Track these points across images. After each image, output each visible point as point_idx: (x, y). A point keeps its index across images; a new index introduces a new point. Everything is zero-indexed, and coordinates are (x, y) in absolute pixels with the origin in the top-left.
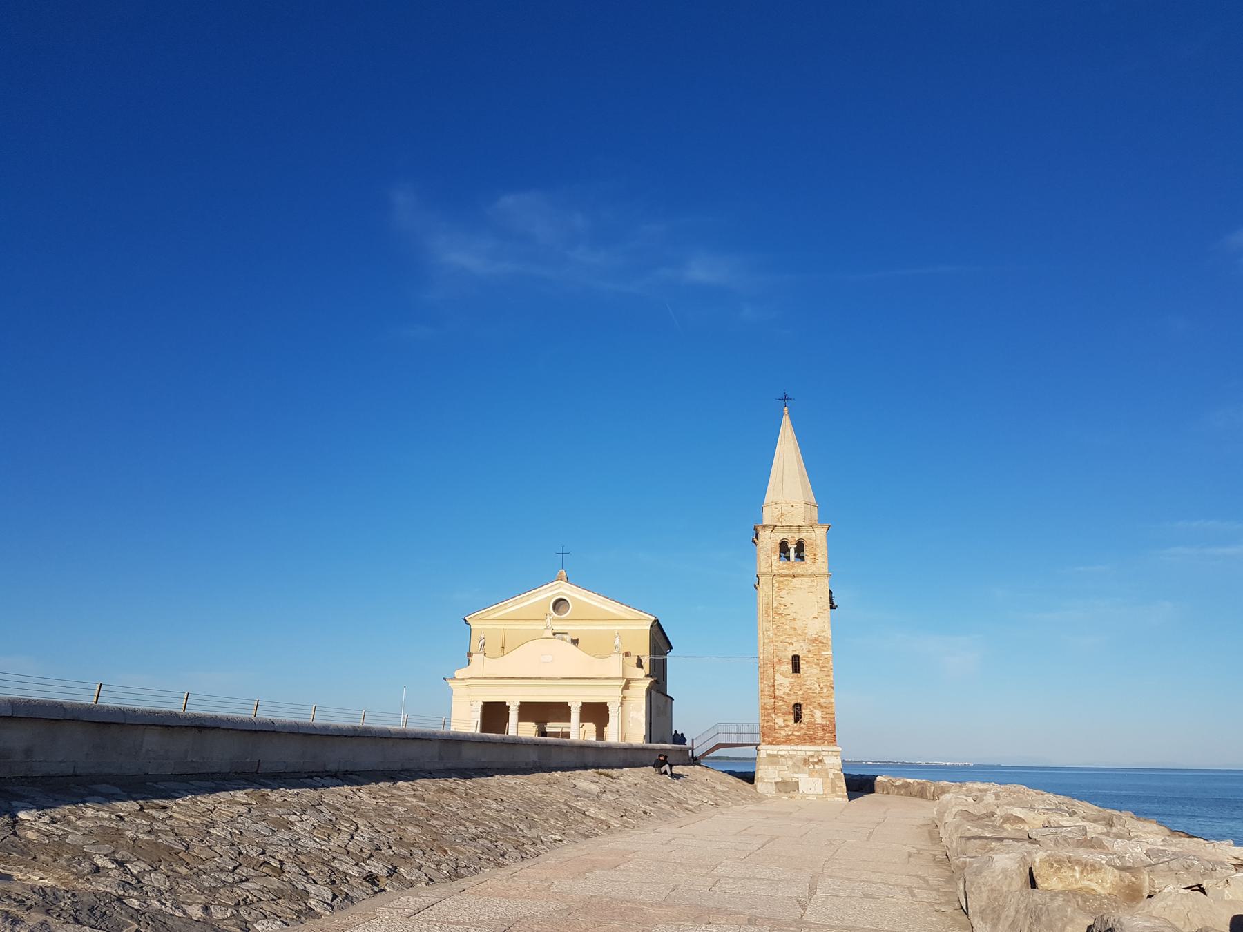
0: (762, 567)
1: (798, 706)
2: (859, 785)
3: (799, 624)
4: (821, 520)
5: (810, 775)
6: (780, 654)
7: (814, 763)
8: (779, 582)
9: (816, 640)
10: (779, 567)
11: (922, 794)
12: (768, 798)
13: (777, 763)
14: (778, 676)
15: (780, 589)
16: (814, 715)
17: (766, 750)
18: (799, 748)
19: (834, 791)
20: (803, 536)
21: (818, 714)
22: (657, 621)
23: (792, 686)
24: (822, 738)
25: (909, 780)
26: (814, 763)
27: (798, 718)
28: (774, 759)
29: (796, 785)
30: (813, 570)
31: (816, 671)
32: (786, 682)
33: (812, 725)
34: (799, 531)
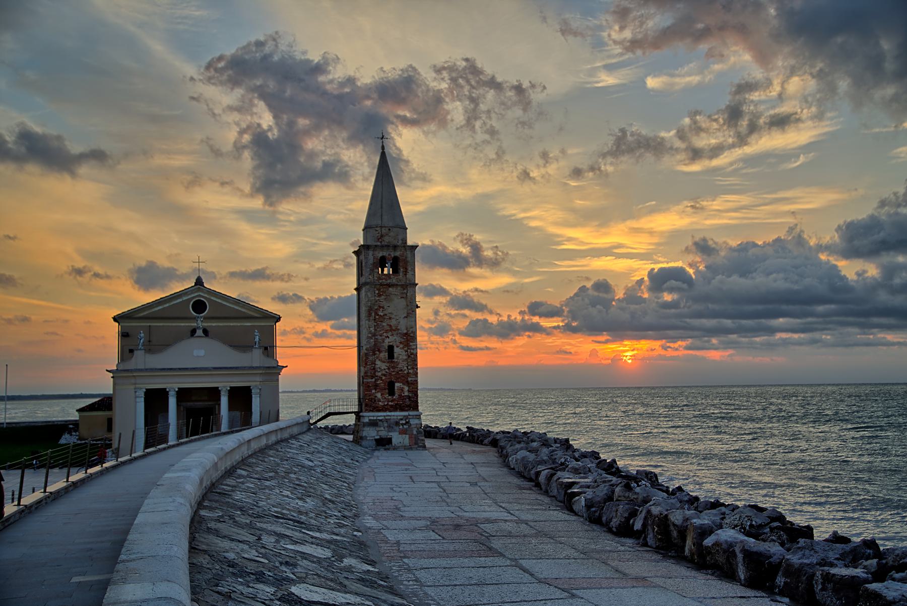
3: (393, 322)
7: (403, 424)
8: (379, 290)
9: (406, 334)
14: (378, 362)
15: (380, 295)
18: (393, 413)
27: (392, 392)
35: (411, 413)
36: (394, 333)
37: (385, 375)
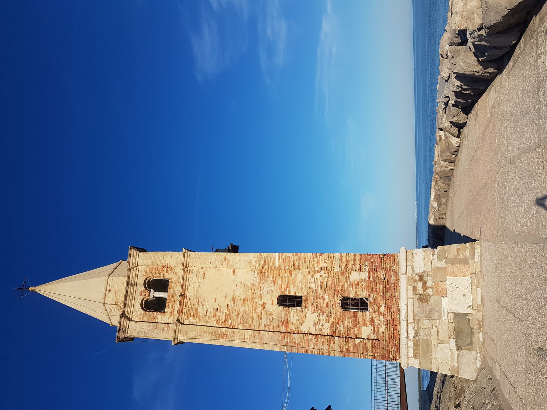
0: (166, 335)
2: (439, 236)
3: (240, 294)
4: (125, 257)
5: (443, 294)
6: (276, 322)
7: (425, 287)
9: (261, 272)
10: (171, 314)
12: (484, 360)
13: (428, 344)
14: (304, 328)
15: (196, 315)
16: (357, 283)
17: (409, 360)
18: (403, 307)
19: (465, 262)
20: (141, 281)
21: (355, 276)
23: (316, 308)
24: (389, 272)
26: (425, 287)
27: (362, 304)
28: (422, 347)
31: (299, 276)
32: (312, 317)
33: (370, 286)
34: (135, 285)
35: (402, 270)
37: (329, 316)
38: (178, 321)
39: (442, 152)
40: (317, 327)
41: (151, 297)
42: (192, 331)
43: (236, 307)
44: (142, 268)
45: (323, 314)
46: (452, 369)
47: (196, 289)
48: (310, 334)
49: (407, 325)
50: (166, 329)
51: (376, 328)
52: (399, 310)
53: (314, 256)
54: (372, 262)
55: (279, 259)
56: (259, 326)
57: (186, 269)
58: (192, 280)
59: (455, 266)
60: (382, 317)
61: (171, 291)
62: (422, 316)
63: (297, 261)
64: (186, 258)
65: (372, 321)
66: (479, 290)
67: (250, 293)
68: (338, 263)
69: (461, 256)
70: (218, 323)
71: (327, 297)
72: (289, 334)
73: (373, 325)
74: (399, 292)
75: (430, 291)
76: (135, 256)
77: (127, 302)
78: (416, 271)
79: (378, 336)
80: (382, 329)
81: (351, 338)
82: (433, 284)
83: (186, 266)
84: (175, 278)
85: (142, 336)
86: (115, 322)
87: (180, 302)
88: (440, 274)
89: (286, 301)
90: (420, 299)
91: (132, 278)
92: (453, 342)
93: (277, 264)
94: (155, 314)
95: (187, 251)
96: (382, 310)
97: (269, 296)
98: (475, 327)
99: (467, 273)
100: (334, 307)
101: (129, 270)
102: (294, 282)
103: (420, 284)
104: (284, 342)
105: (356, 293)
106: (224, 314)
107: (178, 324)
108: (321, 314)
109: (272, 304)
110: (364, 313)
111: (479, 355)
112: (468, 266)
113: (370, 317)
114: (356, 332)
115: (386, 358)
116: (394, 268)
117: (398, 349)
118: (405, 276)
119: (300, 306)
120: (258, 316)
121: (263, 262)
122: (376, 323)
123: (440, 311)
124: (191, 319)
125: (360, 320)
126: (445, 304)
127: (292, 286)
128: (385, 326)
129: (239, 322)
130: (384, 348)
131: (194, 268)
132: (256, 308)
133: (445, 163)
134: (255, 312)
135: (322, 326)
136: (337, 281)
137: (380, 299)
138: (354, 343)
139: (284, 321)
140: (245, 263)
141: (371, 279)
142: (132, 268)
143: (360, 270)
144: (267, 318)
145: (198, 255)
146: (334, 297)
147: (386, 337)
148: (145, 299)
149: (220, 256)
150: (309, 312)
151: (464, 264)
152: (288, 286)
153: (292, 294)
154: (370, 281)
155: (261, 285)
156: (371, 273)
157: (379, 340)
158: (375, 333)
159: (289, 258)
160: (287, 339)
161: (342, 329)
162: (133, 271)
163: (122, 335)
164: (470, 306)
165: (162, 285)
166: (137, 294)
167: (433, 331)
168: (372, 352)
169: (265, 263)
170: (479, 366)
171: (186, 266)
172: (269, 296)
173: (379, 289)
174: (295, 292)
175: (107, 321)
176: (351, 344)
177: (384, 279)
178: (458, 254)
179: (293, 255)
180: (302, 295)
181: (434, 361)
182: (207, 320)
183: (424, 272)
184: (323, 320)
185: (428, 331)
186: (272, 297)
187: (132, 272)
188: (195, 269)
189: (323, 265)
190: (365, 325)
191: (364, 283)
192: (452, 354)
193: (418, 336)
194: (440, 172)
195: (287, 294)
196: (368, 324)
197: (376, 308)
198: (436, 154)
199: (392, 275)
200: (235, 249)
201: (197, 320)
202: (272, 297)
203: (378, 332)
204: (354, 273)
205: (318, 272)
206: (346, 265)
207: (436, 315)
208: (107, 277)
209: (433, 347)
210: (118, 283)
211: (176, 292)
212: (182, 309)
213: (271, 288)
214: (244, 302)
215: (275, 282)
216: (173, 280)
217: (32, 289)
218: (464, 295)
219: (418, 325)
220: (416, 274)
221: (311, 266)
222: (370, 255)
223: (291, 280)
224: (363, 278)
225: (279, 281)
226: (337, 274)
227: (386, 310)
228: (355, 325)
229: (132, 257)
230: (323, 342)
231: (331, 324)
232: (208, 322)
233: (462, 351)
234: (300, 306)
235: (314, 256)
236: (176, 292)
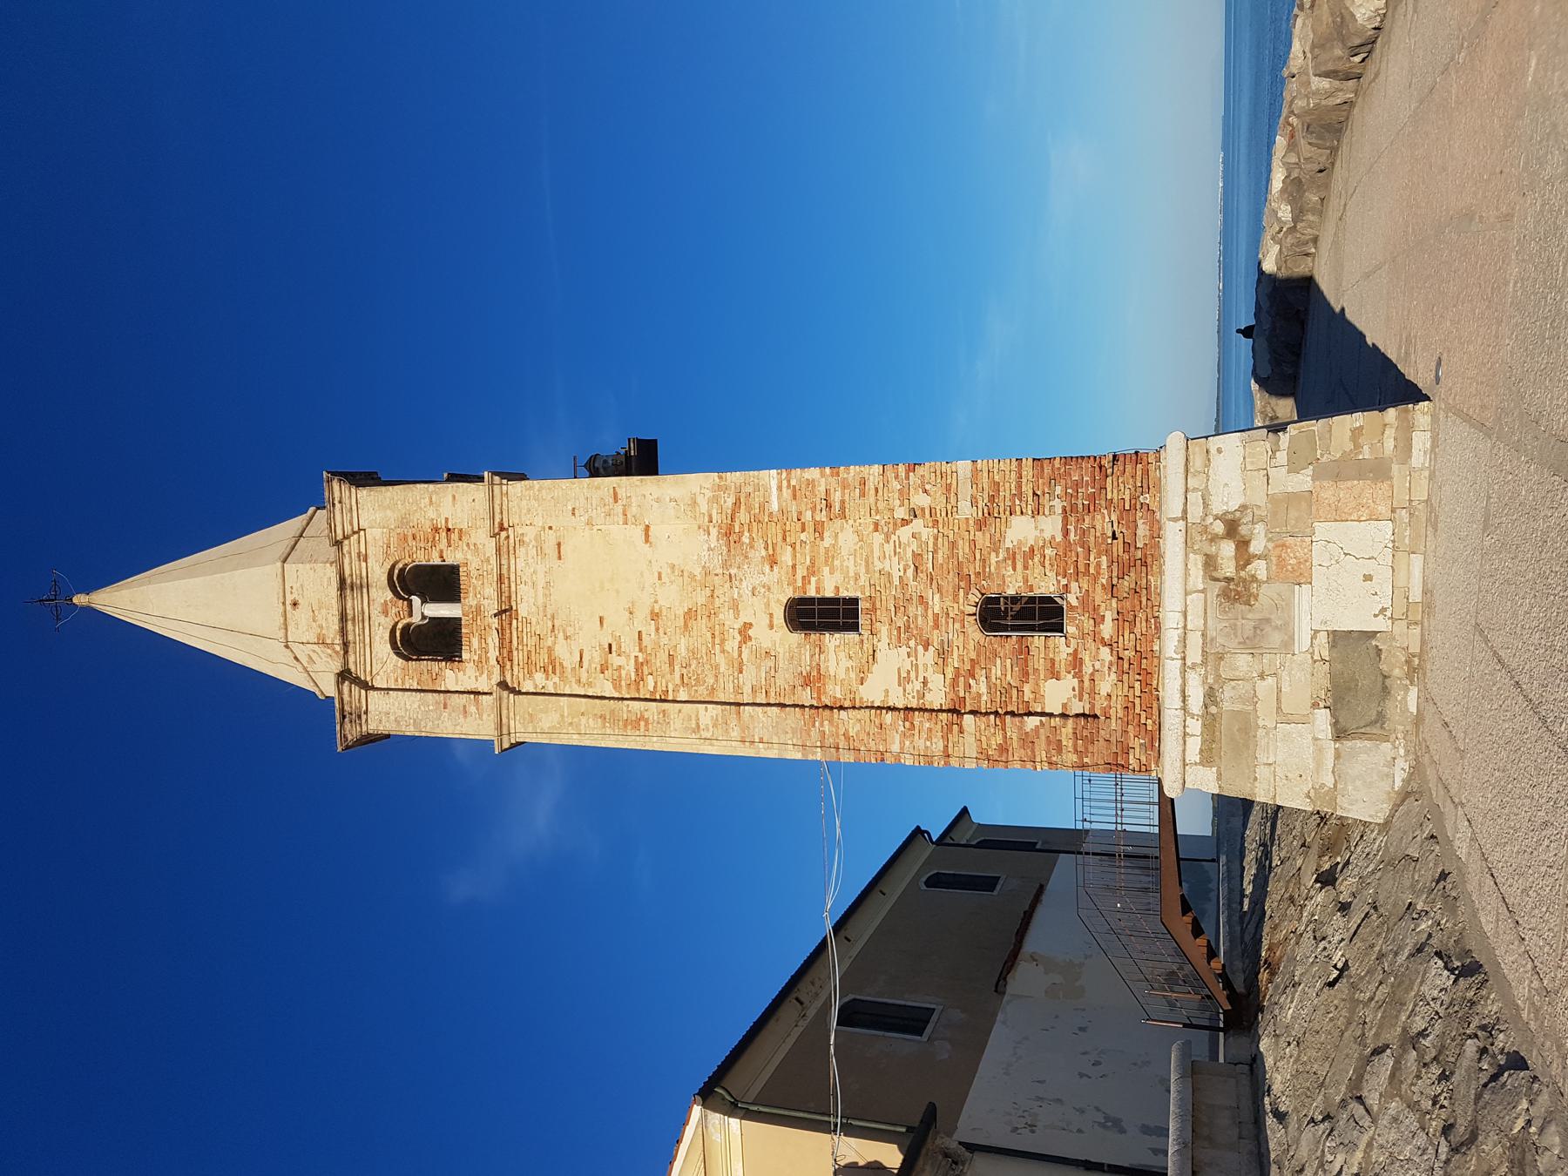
1: (999, 615)
3: (673, 599)
5: (1300, 576)
6: (784, 679)
10: (480, 664)
11: (1330, 128)
12: (1416, 770)
13: (1246, 727)
14: (872, 693)
15: (552, 667)
16: (1029, 546)
18: (1171, 619)
19: (1378, 471)
20: (378, 573)
22: (708, 1094)
23: (905, 633)
24: (1128, 513)
25: (1277, 182)
27: (1043, 615)
29: (1351, 647)
30: (482, 537)
31: (844, 537)
32: (891, 659)
33: (1069, 560)
34: (364, 586)
35: (1173, 506)
36: (724, 593)
37: (943, 654)
38: (503, 685)
39: (1319, 46)
40: (909, 687)
41: (416, 619)
42: (545, 711)
43: (664, 640)
44: (375, 534)
45: (926, 649)
46: (1315, 793)
47: (541, 592)
48: (889, 708)
49: (1183, 672)
50: (473, 709)
51: (1087, 683)
52: (1158, 628)
53: (890, 474)
54: (1077, 485)
55: (780, 488)
56: (738, 689)
57: (503, 534)
58: (524, 564)
59: (1342, 485)
60: (1105, 651)
61: (469, 600)
62: (1232, 644)
63: (838, 494)
64: (497, 502)
65: (1076, 662)
66: (1417, 561)
67: (701, 598)
68: (966, 491)
69: (1366, 453)
70: (617, 686)
71: (937, 597)
72: (827, 712)
73: (1079, 675)
74: (1161, 573)
75: (1259, 568)
76: (346, 500)
77: (350, 638)
78: (1218, 507)
79: (1093, 706)
80: (1106, 685)
81: (1012, 714)
82: (1270, 545)
83: (501, 524)
84: (474, 563)
85: (410, 731)
86: (328, 687)
87: (501, 632)
88: (1293, 514)
89: (811, 614)
90: (1225, 594)
91: (352, 567)
92: (1323, 718)
93: (775, 507)
94: (435, 666)
95: (497, 479)
96: (1107, 629)
97: (758, 602)
98: (1397, 672)
99: (1383, 509)
100: (957, 626)
101: (338, 544)
102: (830, 557)
103: (1228, 549)
104: (814, 733)
105: (1026, 581)
106: (632, 661)
107: (505, 693)
108: (920, 648)
109: (771, 627)
110: (1051, 642)
111: (1402, 752)
112: (1386, 485)
113: (1070, 650)
114: (1028, 696)
115: (1117, 765)
116: (1146, 498)
117: (1154, 740)
118: (1181, 524)
119: (854, 627)
120: (731, 663)
121: (730, 501)
122: (1087, 669)
123: (1287, 628)
124: (539, 677)
125: (1038, 662)
126: (1305, 607)
127: (826, 570)
128: (1113, 676)
129: (678, 681)
130: (1113, 739)
131: (525, 529)
132: (723, 641)
133: (1325, 84)
134: (723, 651)
135: (925, 683)
136: (963, 549)
137: (1099, 596)
138: (1020, 728)
139: (809, 674)
140: (675, 503)
141: (1072, 536)
142: (346, 537)
143: (1037, 512)
144: (759, 668)
145: (531, 488)
146: (956, 596)
147: (1117, 709)
148: (400, 626)
149: (598, 488)
150: (882, 646)
151: (1375, 479)
152: (812, 570)
153: (829, 594)
154: (1068, 546)
155: (733, 571)
156: (1072, 519)
157: (1095, 716)
158: (1086, 696)
159: (811, 483)
160: (822, 724)
161: (983, 689)
162: (351, 546)
163: (352, 732)
164: (1384, 610)
165: (440, 582)
166: (374, 613)
167: (1265, 687)
168: (1076, 751)
169: (737, 504)
170: (1398, 784)
171: (501, 524)
172: (758, 602)
173: (1099, 565)
174: (837, 588)
175: (309, 687)
176: (1012, 733)
177: (1114, 537)
178: (1358, 446)
179: (823, 475)
180: (859, 594)
181: (1262, 772)
182: (583, 680)
183: (1243, 508)
184: (925, 666)
185: (1248, 686)
186: (768, 605)
187: (346, 549)
188: (530, 534)
189: (920, 500)
190: (1056, 676)
191: (1049, 552)
192: (1320, 750)
193: (1216, 704)
194: (1308, 112)
195: (812, 593)
196: (1063, 673)
197: (1088, 625)
198: (1296, 47)
199: (1140, 522)
200: (643, 460)
201: (556, 679)
202: (768, 605)
203: (1093, 693)
204: (1016, 520)
205: (905, 522)
206: (992, 498)
207: (1276, 638)
208: (279, 564)
209: (1260, 733)
210: (314, 581)
211: (486, 602)
212: (511, 652)
213: (765, 579)
214: (686, 625)
215: (773, 562)
216: (473, 566)
217: (80, 599)
218: (1368, 578)
219: (1217, 669)
220: (1216, 518)
221: (881, 505)
222: (1067, 460)
223: (822, 551)
224: (1047, 536)
225: (786, 557)
226: (963, 526)
227: (1119, 631)
228: (1025, 676)
229: (338, 506)
230: (930, 730)
231: (949, 676)
232: (590, 684)
233: (1349, 744)
234: (854, 627)
235: (890, 474)
236: (486, 602)
